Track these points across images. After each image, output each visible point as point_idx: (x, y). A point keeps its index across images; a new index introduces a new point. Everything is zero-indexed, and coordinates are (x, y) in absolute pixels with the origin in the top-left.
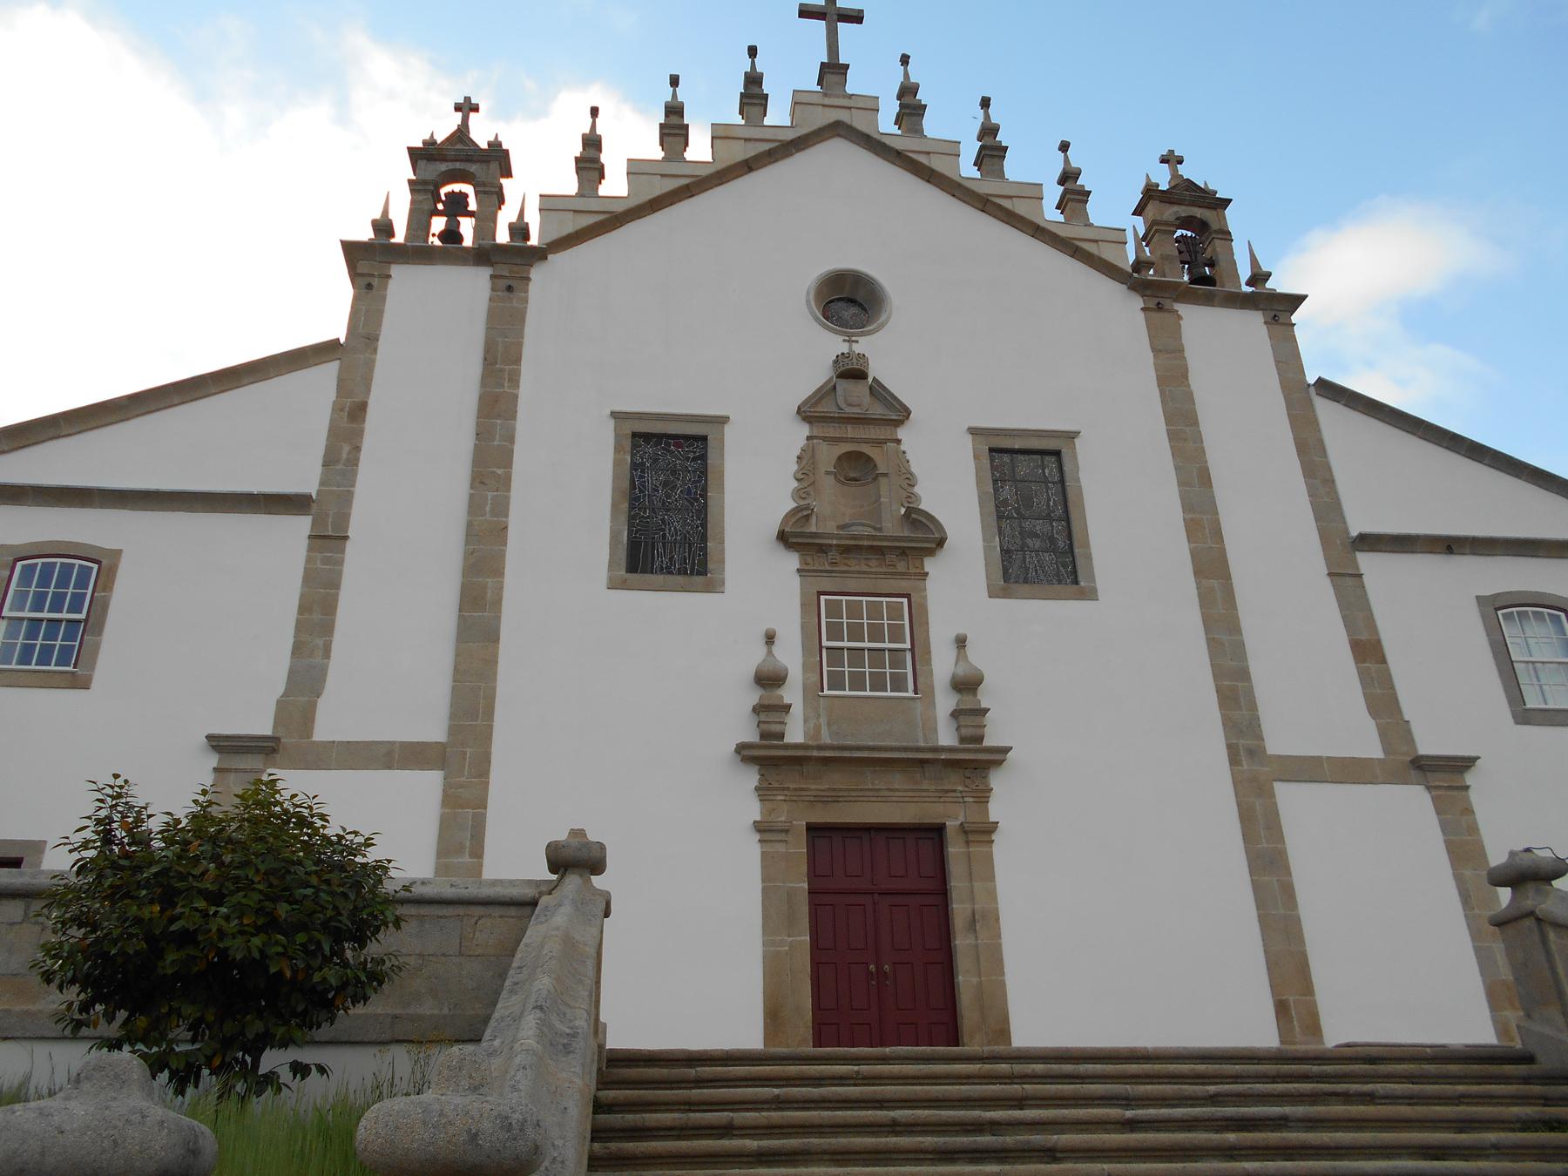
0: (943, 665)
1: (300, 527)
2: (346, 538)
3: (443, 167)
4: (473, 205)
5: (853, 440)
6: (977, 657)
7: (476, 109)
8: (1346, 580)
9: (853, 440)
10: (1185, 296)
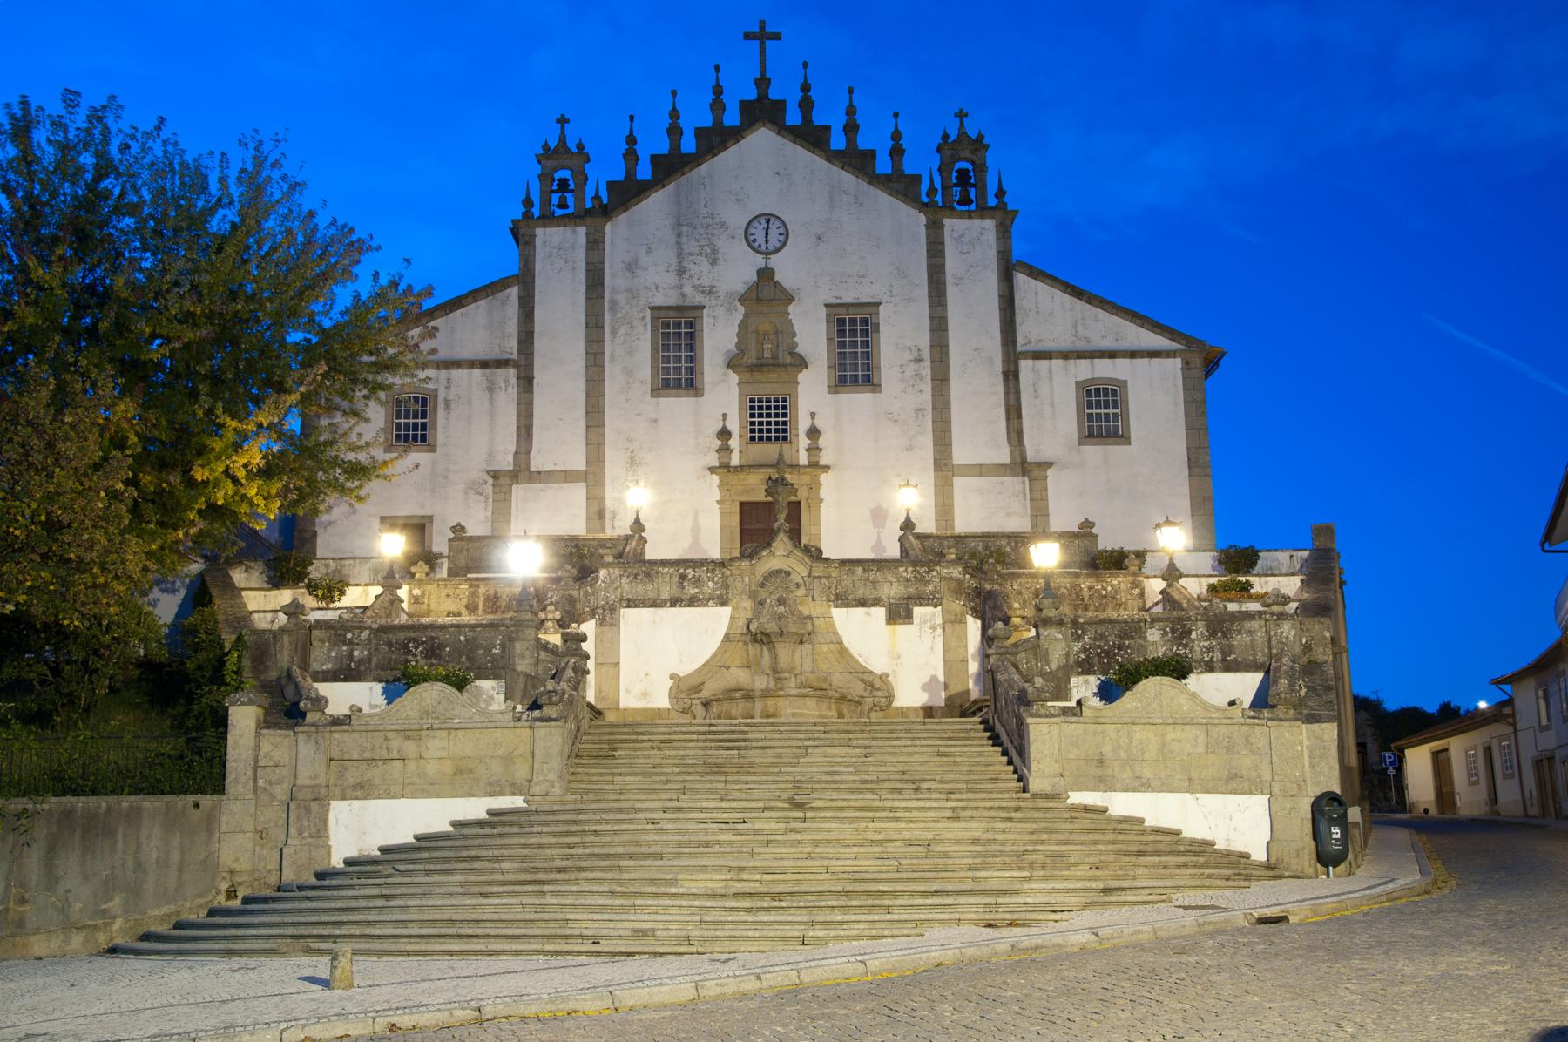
0: (803, 424)
4: (572, 186)
6: (819, 423)
7: (568, 121)
8: (1011, 376)
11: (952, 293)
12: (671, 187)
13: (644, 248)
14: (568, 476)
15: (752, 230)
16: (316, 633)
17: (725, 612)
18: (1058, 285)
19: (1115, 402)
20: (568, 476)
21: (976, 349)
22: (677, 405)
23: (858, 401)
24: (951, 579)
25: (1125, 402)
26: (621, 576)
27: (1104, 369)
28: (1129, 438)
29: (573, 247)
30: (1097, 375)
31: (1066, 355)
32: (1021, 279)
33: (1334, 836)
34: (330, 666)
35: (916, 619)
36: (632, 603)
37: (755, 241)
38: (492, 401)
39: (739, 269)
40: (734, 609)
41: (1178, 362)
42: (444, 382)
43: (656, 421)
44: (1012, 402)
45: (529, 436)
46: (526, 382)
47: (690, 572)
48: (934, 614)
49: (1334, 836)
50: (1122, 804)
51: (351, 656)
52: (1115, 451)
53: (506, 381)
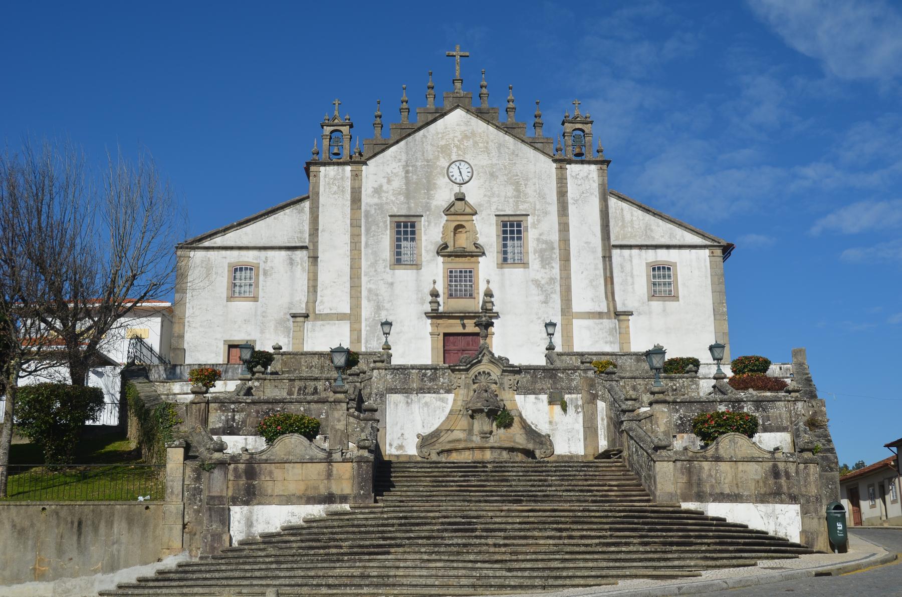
0: (482, 288)
2: (318, 257)
3: (332, 128)
5: (458, 221)
6: (491, 286)
8: (607, 258)
9: (458, 221)
10: (570, 162)
11: (572, 209)
12: (402, 143)
13: (385, 180)
14: (341, 317)
15: (451, 170)
16: (212, 405)
17: (451, 397)
18: (634, 206)
19: (669, 277)
20: (341, 317)
21: (586, 243)
22: (404, 275)
23: (515, 274)
25: (676, 275)
26: (386, 374)
27: (663, 256)
28: (678, 297)
29: (342, 178)
30: (658, 259)
31: (640, 247)
32: (613, 202)
33: (839, 528)
34: (221, 425)
37: (453, 176)
39: (444, 195)
40: (456, 395)
41: (707, 252)
44: (608, 274)
45: (315, 291)
46: (314, 259)
47: (429, 372)
49: (839, 528)
50: (714, 510)
51: (233, 419)
52: (671, 305)
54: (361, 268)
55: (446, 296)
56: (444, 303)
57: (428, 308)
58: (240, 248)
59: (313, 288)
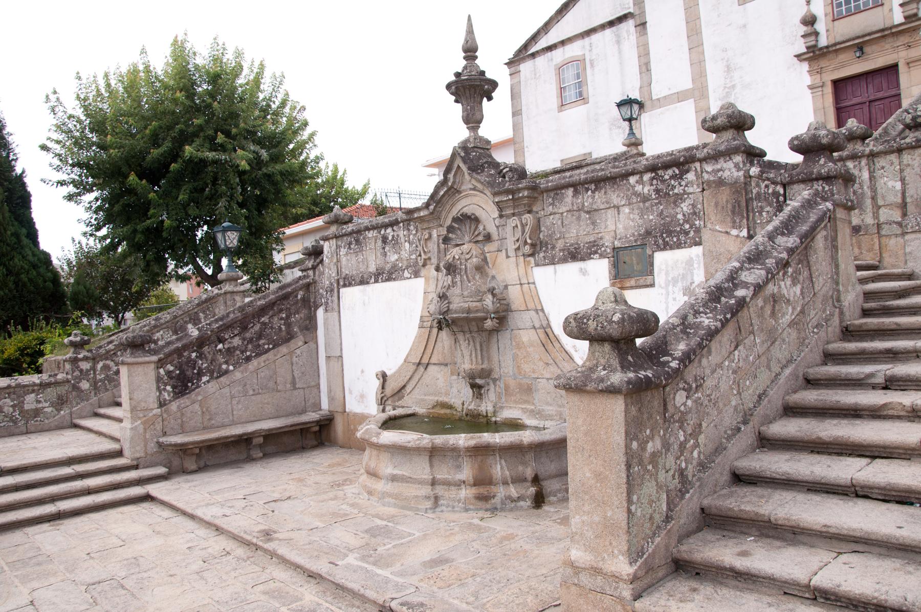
1: (630, 23)
24: (721, 183)
35: (659, 277)
36: (348, 282)
38: (620, 52)
42: (588, 47)
43: (745, 26)
45: (649, 70)
46: (643, 25)
48: (690, 262)
53: (628, 31)
54: (699, 18)
55: (830, 18)
56: (827, 31)
57: (801, 47)
58: (563, 43)
59: (645, 67)
